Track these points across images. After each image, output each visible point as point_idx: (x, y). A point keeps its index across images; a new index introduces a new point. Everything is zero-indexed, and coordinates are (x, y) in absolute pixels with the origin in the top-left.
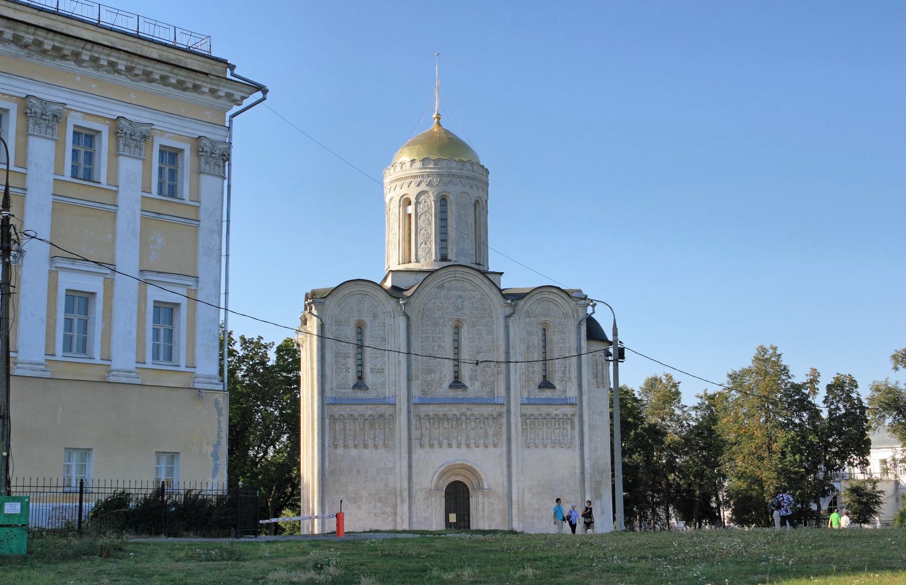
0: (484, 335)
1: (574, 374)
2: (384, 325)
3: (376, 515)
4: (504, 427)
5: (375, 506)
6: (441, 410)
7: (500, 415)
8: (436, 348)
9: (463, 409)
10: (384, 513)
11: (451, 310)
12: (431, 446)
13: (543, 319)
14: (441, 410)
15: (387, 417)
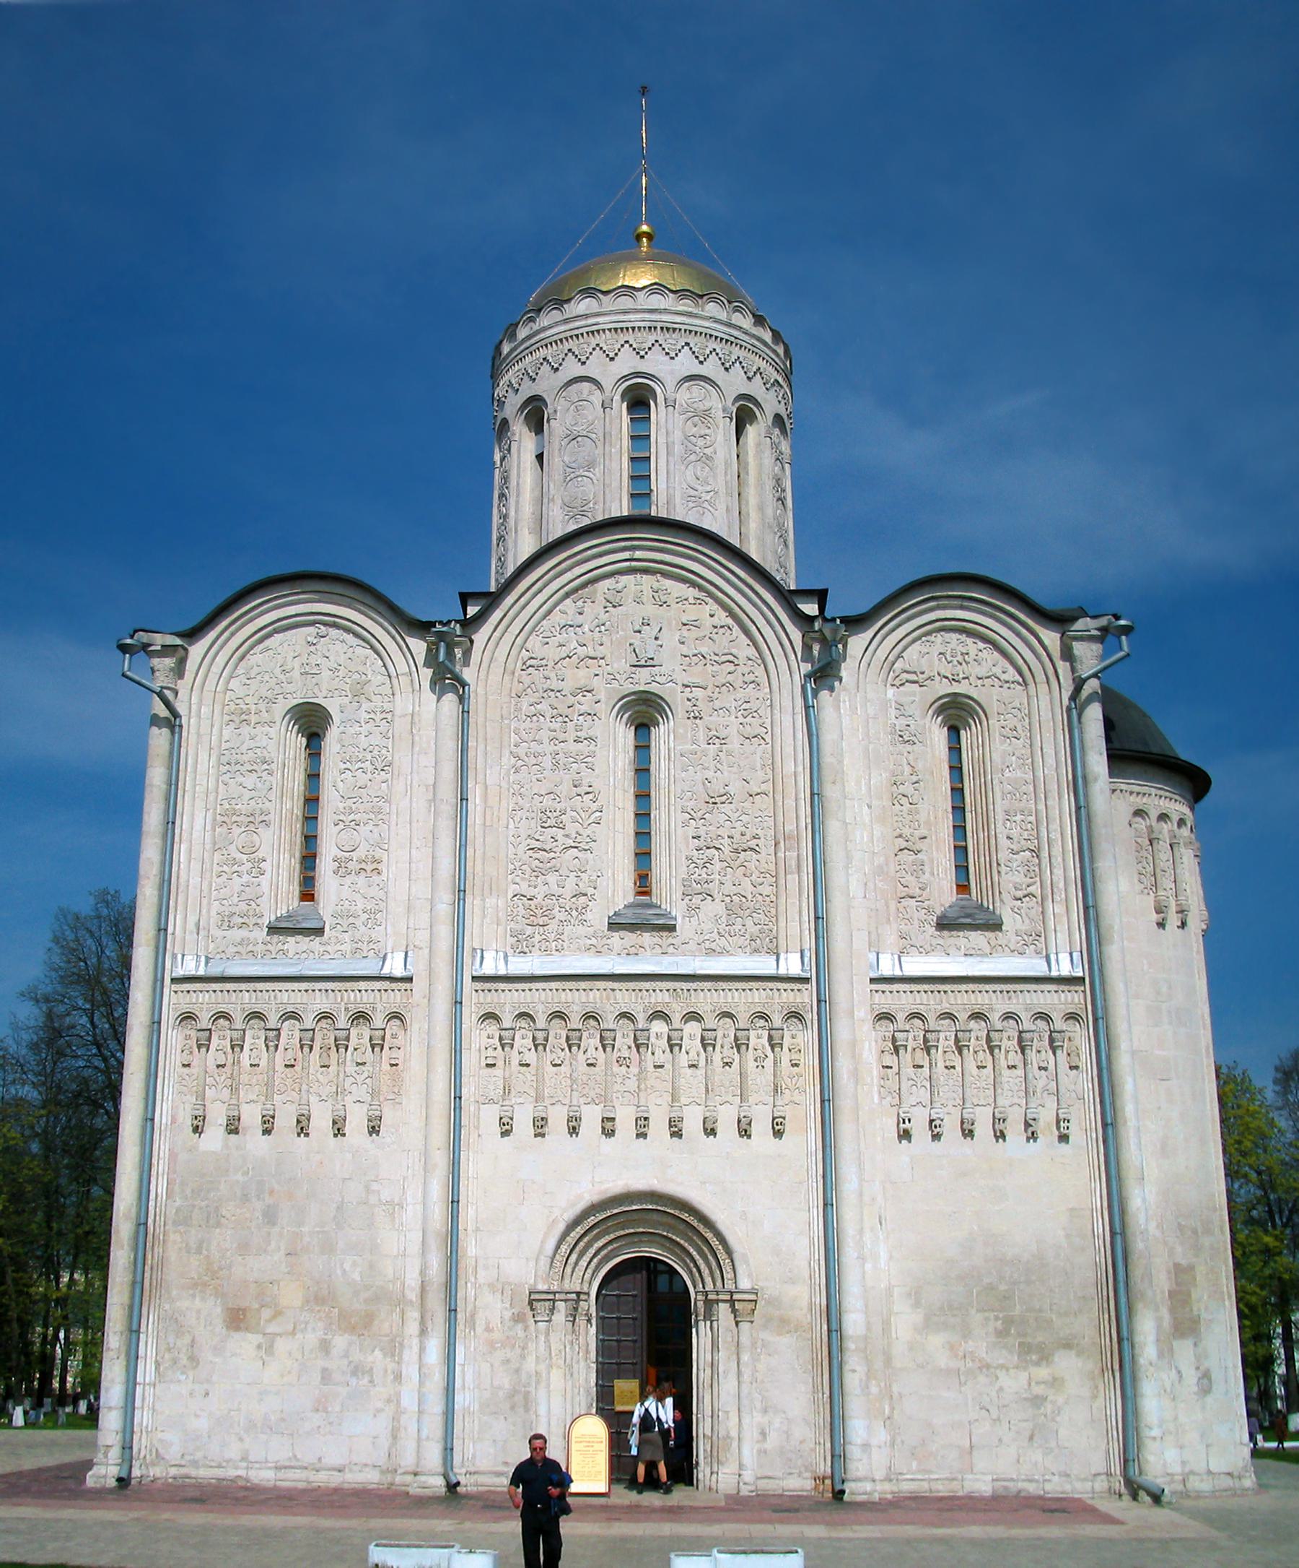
0: (734, 743)
1: (1064, 866)
2: (388, 716)
3: (326, 1376)
4: (810, 1060)
5: (325, 1347)
6: (575, 1000)
7: (795, 1015)
8: (565, 789)
9: (660, 996)
10: (356, 1370)
11: (621, 664)
12: (540, 1126)
13: (946, 688)
14: (575, 1000)
15: (378, 1021)
